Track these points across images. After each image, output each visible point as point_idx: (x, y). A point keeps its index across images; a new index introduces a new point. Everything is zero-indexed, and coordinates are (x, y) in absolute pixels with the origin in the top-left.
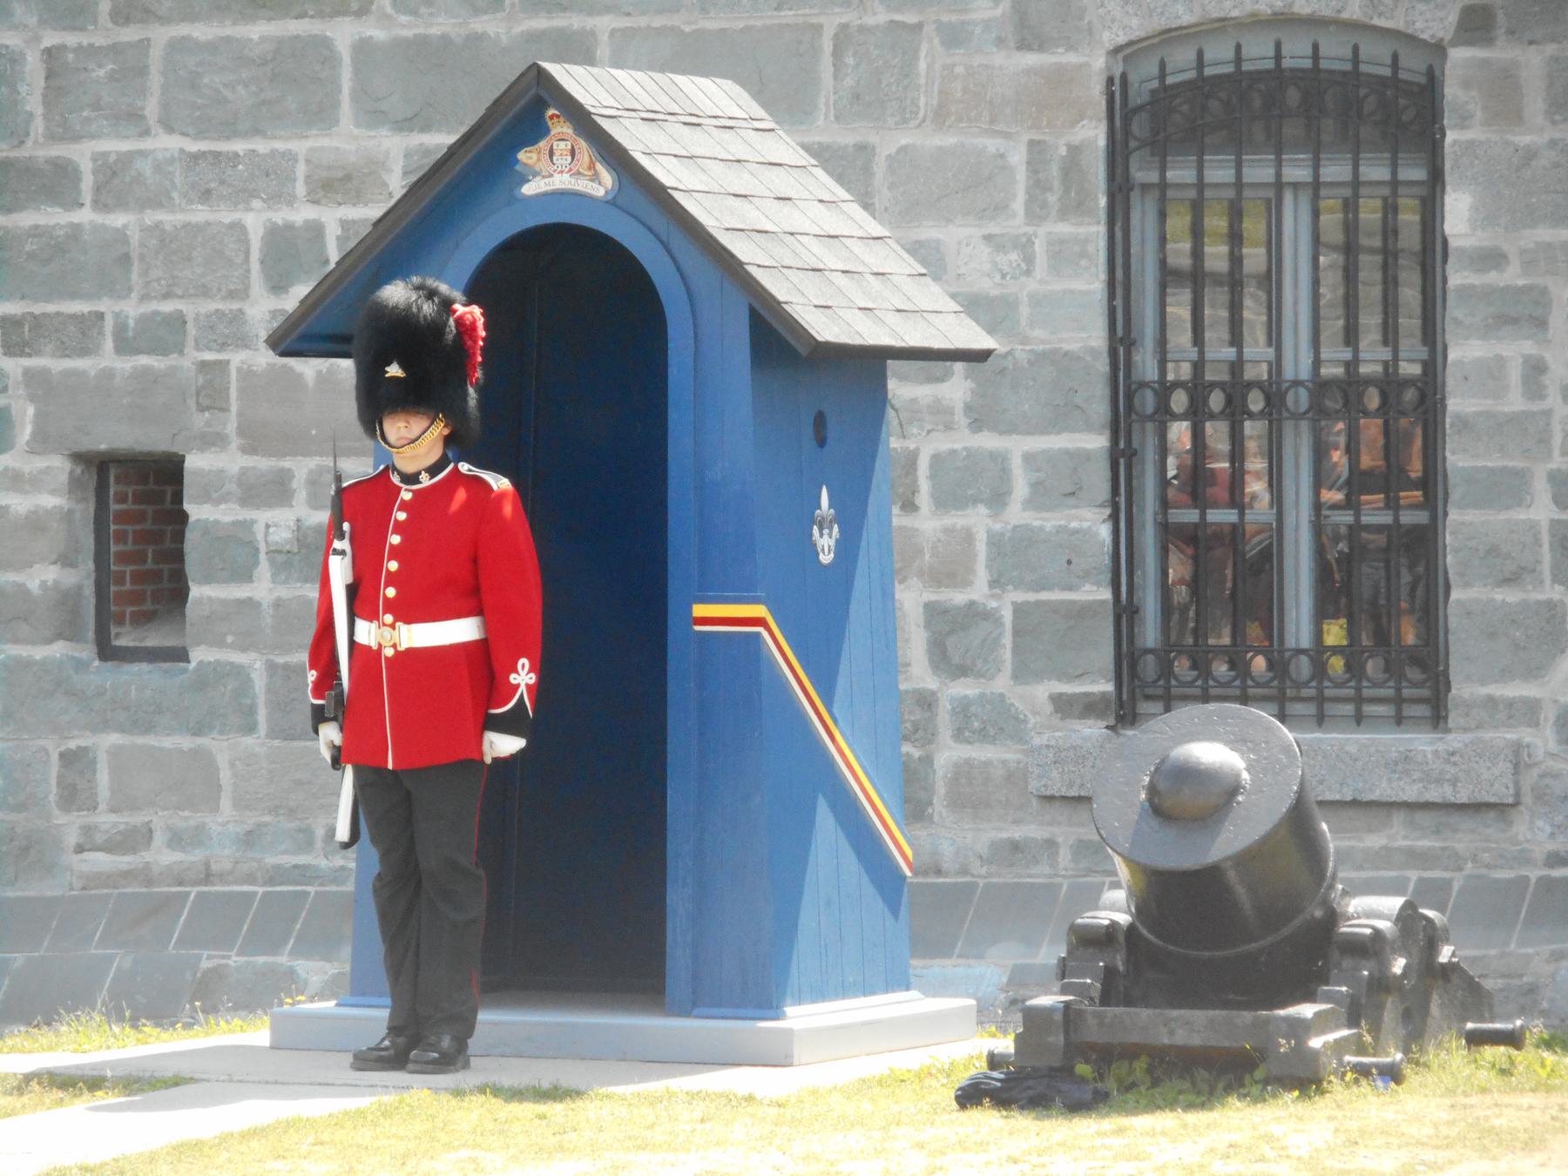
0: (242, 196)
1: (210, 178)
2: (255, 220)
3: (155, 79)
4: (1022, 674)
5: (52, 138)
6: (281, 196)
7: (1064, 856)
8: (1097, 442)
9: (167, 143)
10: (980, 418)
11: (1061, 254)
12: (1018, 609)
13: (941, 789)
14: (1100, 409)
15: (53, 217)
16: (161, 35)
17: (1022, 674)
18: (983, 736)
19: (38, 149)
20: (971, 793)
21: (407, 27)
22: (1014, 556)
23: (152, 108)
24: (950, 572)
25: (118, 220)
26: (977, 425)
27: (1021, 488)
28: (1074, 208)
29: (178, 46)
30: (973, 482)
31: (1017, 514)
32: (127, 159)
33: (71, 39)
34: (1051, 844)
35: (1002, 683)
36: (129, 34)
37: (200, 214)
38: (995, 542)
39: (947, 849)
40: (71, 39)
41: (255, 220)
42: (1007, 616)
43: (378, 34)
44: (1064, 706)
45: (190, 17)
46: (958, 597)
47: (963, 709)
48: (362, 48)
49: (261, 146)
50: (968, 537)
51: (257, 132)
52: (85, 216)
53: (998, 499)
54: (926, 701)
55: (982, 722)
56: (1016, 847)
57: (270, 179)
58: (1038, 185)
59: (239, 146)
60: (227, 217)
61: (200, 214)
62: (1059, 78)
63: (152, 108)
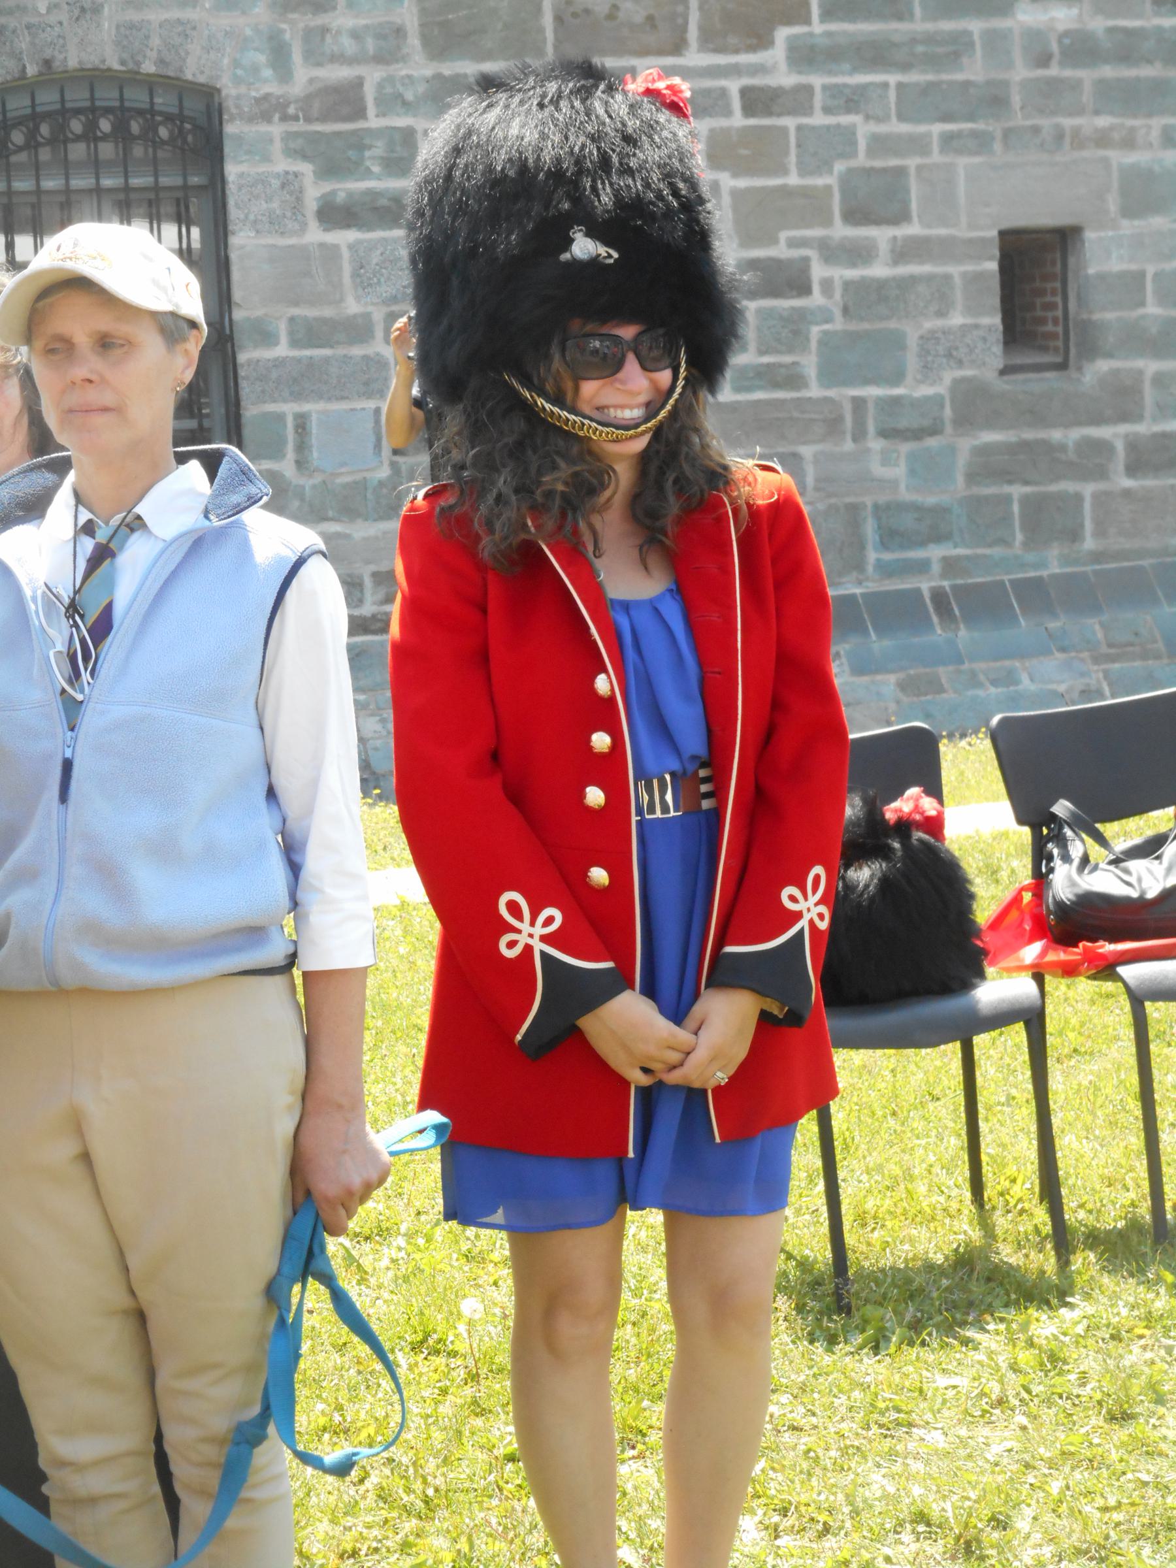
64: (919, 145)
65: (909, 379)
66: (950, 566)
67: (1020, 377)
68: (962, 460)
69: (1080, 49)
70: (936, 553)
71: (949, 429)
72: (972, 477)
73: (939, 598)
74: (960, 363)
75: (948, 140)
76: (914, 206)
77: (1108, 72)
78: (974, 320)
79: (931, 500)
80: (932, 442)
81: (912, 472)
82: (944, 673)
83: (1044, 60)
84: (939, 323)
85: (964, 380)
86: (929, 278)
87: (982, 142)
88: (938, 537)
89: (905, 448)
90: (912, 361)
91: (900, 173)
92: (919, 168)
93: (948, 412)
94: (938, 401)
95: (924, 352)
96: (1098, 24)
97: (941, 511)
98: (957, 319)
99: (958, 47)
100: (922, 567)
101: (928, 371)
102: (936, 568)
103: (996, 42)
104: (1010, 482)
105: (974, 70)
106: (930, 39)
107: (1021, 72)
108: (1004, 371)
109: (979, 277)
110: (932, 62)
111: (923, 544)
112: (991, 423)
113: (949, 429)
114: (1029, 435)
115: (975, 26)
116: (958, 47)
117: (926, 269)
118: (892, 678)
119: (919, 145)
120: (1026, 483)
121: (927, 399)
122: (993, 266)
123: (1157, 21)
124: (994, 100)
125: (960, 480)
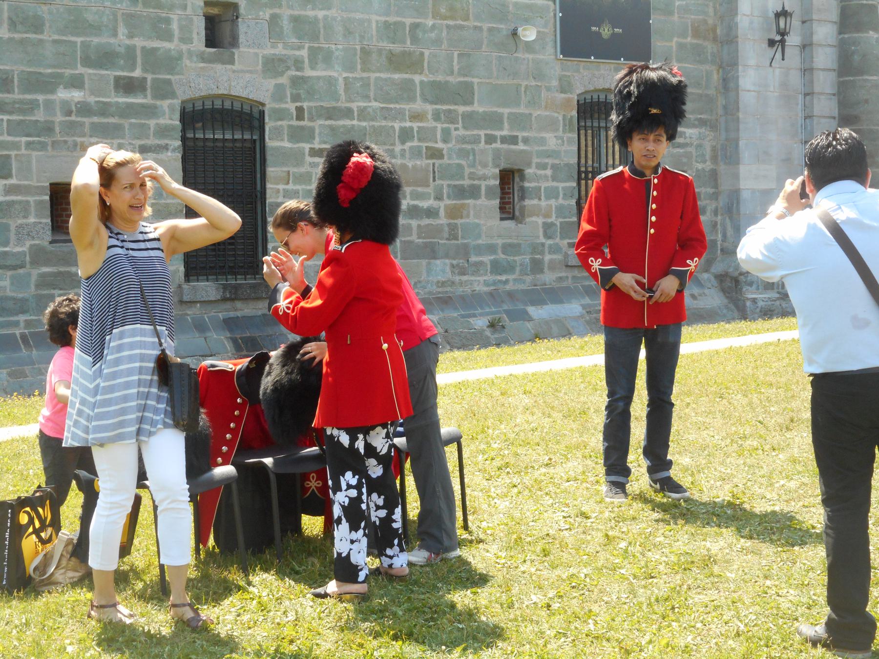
0: (394, 119)
1: (386, 114)
2: (397, 125)
3: (372, 87)
4: (562, 238)
5: (347, 101)
6: (403, 120)
7: (570, 279)
8: (575, 184)
9: (375, 104)
10: (554, 178)
11: (570, 141)
12: (561, 223)
13: (546, 265)
14: (576, 177)
15: (348, 122)
16: (373, 76)
17: (562, 238)
18: (554, 253)
19: (343, 104)
20: (552, 267)
21: (432, 78)
22: (560, 210)
23: (372, 94)
24: (547, 215)
25: (364, 124)
26: (553, 181)
27: (561, 195)
28: (571, 131)
29: (377, 79)
30: (552, 194)
31: (561, 201)
32: (365, 108)
33: (350, 75)
34: (567, 277)
35: (558, 240)
36: (365, 75)
37: (384, 123)
38: (556, 207)
39: (547, 279)
40: (350, 75)
41: (397, 125)
42: (558, 224)
43: (425, 79)
44: (570, 245)
45: (380, 72)
46: (549, 220)
47: (550, 246)
48: (422, 82)
49: (398, 106)
50: (551, 206)
51: (397, 102)
52: (355, 122)
53: (557, 198)
54: (543, 245)
55: (555, 249)
56: (561, 278)
57: (399, 115)
58: (565, 125)
59: (392, 106)
60: (390, 124)
61: (384, 123)
62: (569, 100)
63: (372, 94)
64: (16, 146)
65: (11, 244)
66: (28, 324)
67: (58, 245)
68: (34, 278)
69: (84, 109)
70: (22, 318)
71: (28, 266)
72: (38, 286)
73: (24, 337)
74: (33, 238)
75: (29, 145)
76: (14, 171)
77: (96, 119)
78: (39, 220)
79: (20, 296)
80: (21, 271)
81: (12, 284)
82: (27, 369)
83: (69, 113)
84: (25, 221)
85: (34, 245)
86: (20, 202)
87: (43, 146)
88: (23, 312)
89: (9, 273)
90: (12, 236)
91: (8, 157)
92: (16, 155)
93: (28, 258)
94: (23, 253)
95: (18, 233)
96: (92, 100)
97: (24, 300)
98: (32, 220)
99: (33, 106)
100: (16, 324)
101: (19, 241)
102: (22, 325)
103: (49, 105)
104: (54, 289)
105: (40, 116)
106: (21, 102)
107: (59, 118)
108: (51, 243)
109: (42, 202)
110: (22, 111)
111: (17, 314)
112: (46, 265)
113: (28, 266)
114: (62, 269)
115: (41, 98)
116: (33, 106)
117: (19, 198)
118: (5, 371)
119: (16, 146)
120: (61, 289)
121: (19, 253)
122: (47, 198)
123: (116, 99)
124: (48, 129)
125: (33, 287)
